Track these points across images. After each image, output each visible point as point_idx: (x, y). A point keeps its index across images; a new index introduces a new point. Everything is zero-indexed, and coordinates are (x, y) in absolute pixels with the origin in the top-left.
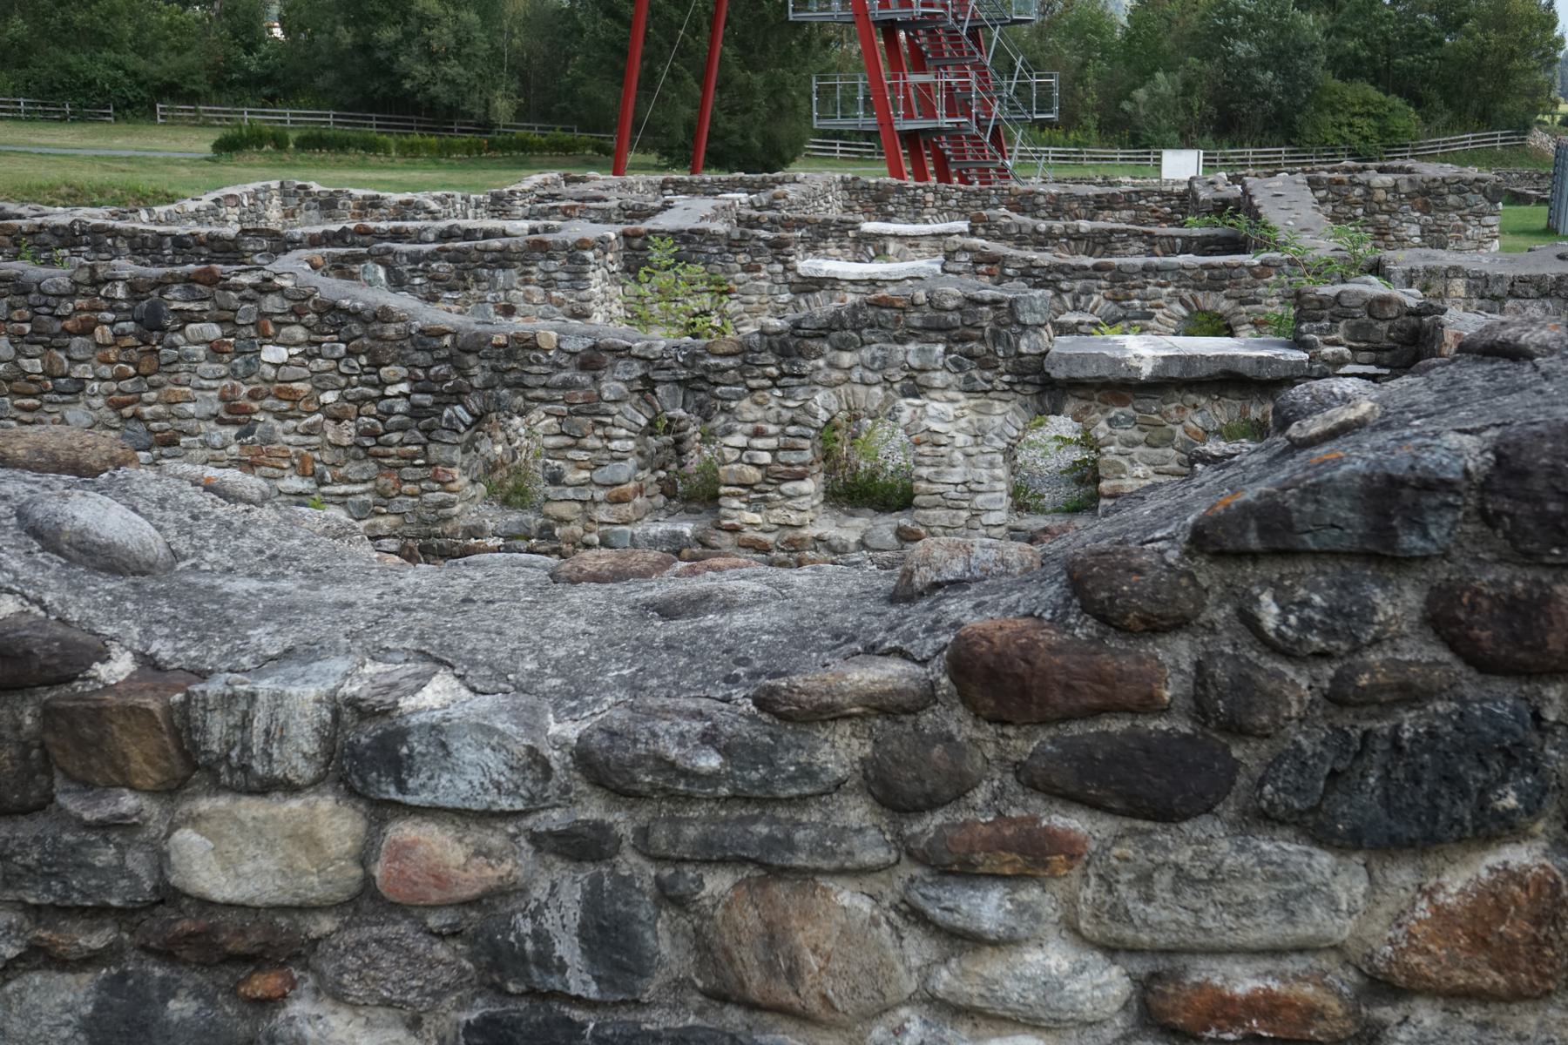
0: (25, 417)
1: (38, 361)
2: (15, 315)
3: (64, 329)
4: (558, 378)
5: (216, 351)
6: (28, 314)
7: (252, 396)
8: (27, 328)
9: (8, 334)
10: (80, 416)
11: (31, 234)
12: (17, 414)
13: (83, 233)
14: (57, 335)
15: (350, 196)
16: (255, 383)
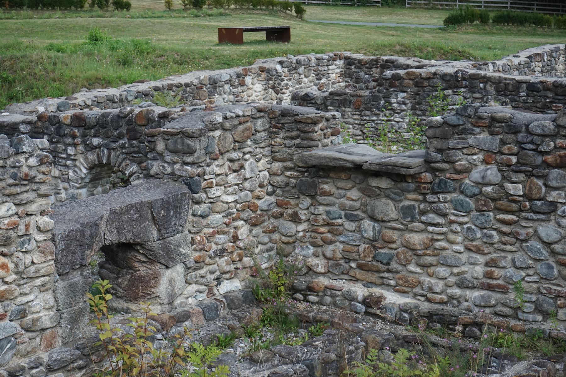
0: (505, 229)
1: (520, 186)
2: (505, 149)
3: (544, 162)
6: (516, 149)
8: (514, 159)
9: (497, 163)
10: (551, 232)
11: (428, 79)
12: (498, 225)
13: (464, 79)
14: (538, 167)
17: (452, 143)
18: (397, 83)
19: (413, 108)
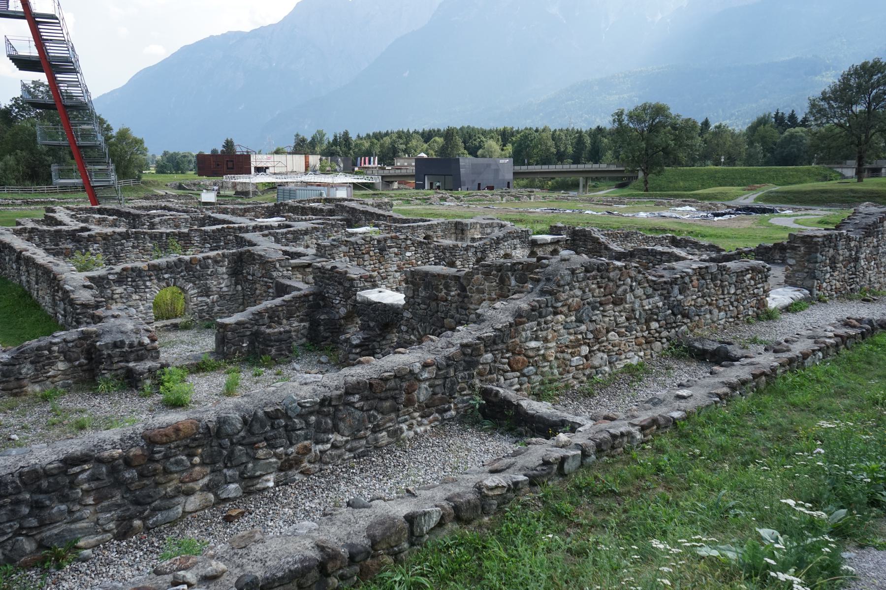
4: (462, 253)
5: (396, 254)
7: (404, 265)
15: (94, 218)
16: (404, 261)
17: (334, 251)
18: (92, 239)
19: (104, 252)
